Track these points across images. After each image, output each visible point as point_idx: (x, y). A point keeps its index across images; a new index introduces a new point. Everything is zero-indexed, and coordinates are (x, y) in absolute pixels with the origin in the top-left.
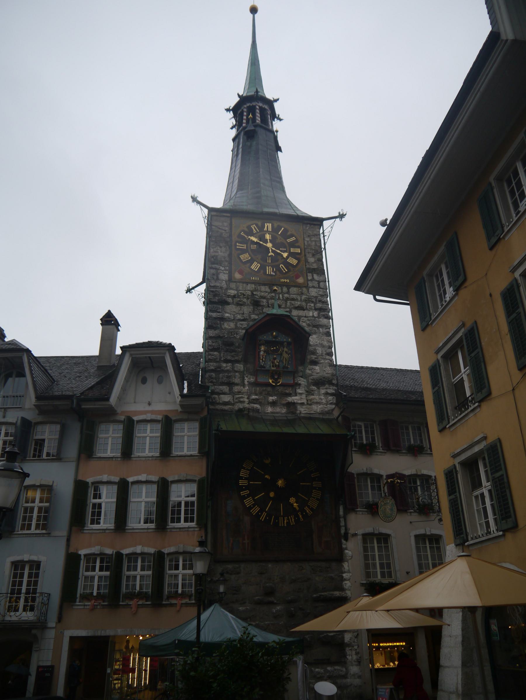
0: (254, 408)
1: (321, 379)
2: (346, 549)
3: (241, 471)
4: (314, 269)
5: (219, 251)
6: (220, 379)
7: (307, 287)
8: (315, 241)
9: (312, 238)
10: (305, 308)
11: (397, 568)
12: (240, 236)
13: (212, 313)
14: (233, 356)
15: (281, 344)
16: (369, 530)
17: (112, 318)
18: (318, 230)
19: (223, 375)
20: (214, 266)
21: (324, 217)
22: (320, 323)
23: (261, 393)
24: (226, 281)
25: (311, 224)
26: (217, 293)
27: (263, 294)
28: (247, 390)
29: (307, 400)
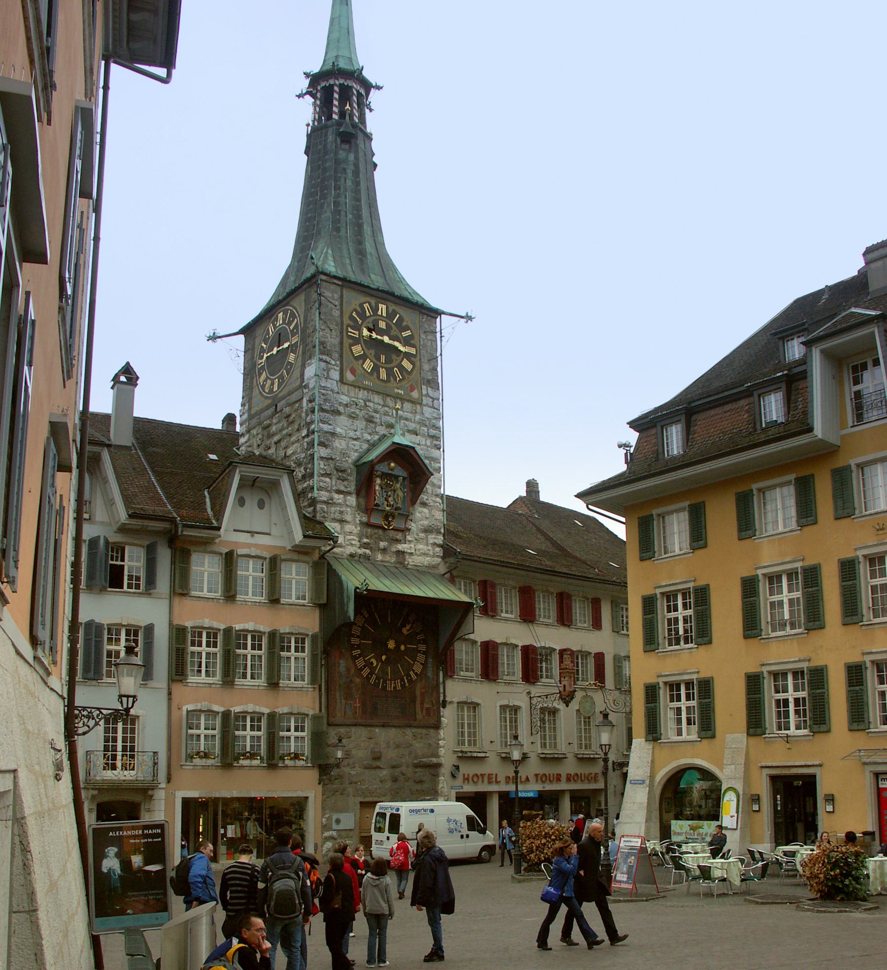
4: (429, 381)
7: (421, 404)
8: (432, 341)
11: (483, 737)
12: (351, 318)
14: (346, 487)
15: (396, 477)
16: (463, 699)
17: (132, 375)
20: (324, 357)
25: (428, 315)
27: (376, 406)
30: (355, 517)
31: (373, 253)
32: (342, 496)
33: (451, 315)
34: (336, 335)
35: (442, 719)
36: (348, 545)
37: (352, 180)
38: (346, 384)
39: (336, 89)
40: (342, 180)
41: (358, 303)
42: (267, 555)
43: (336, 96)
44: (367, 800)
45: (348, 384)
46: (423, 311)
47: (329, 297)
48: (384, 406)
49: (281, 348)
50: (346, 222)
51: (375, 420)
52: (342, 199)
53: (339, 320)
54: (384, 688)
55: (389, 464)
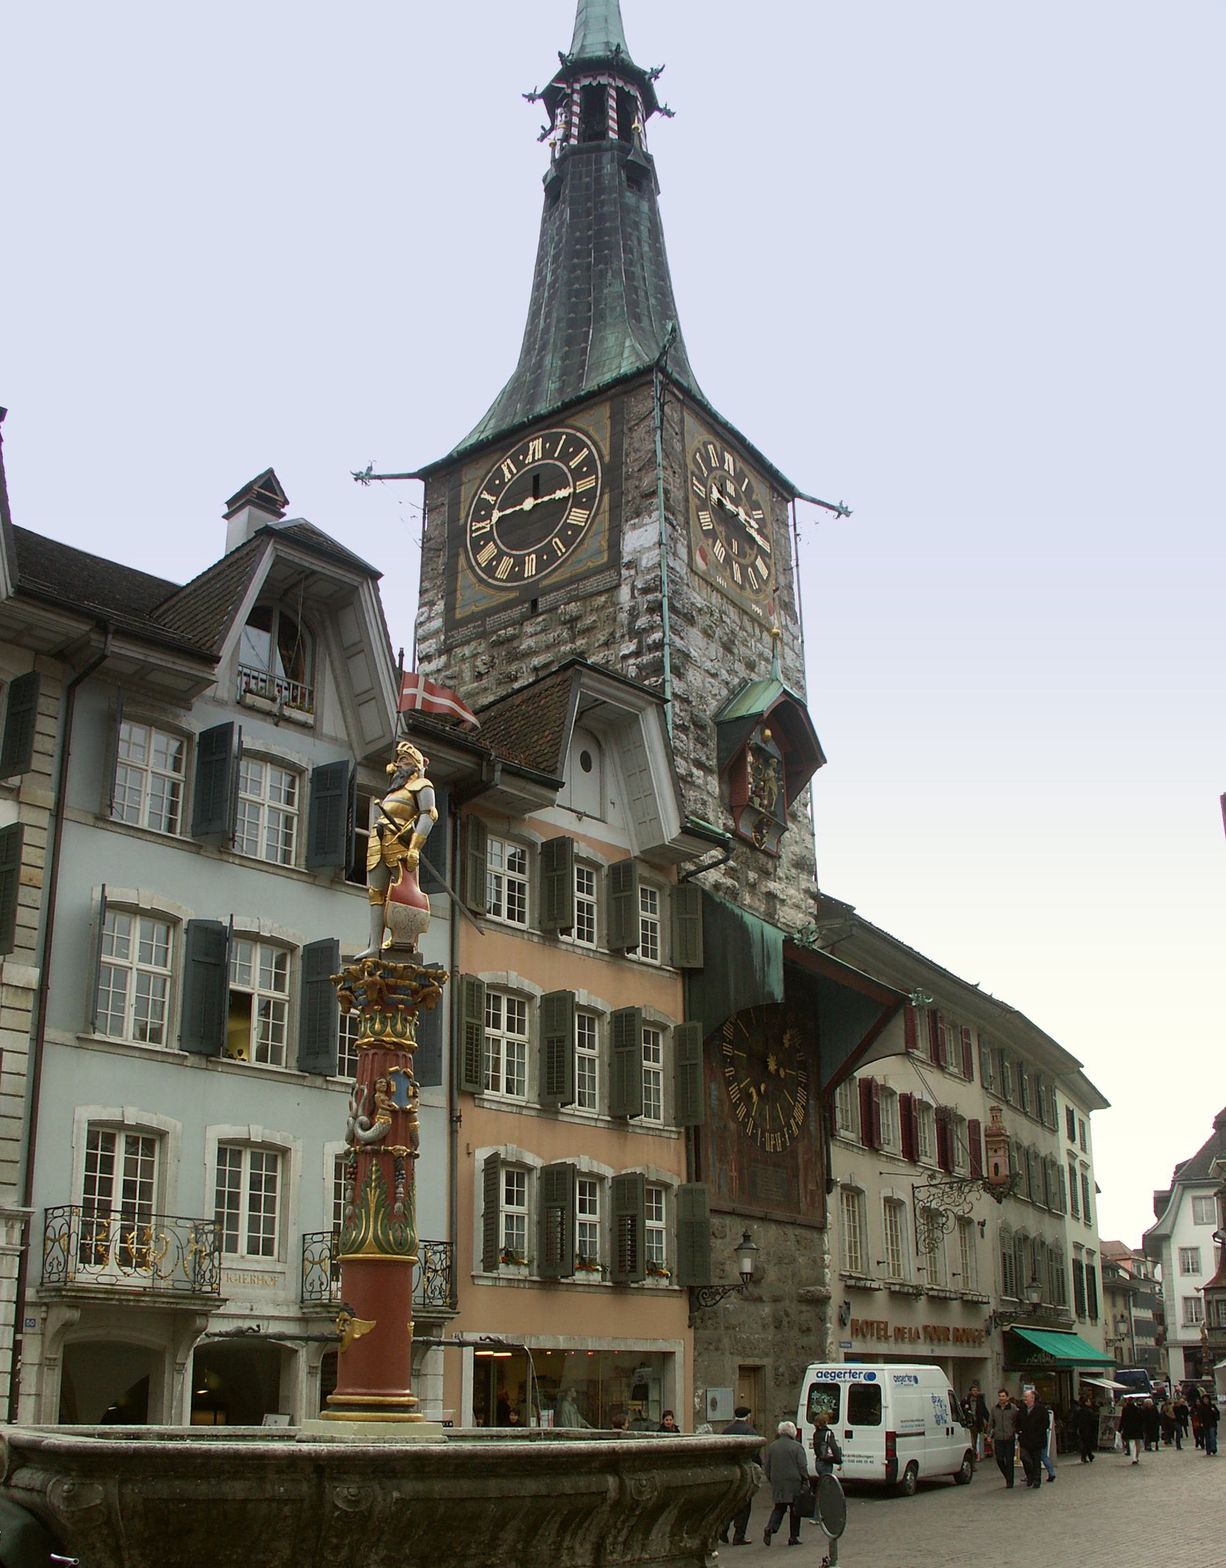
6: (691, 803)
17: (277, 495)
21: (800, 487)
33: (813, 501)
37: (649, 244)
39: (613, 93)
40: (635, 239)
43: (612, 103)
49: (539, 501)
52: (637, 270)
55: (762, 733)
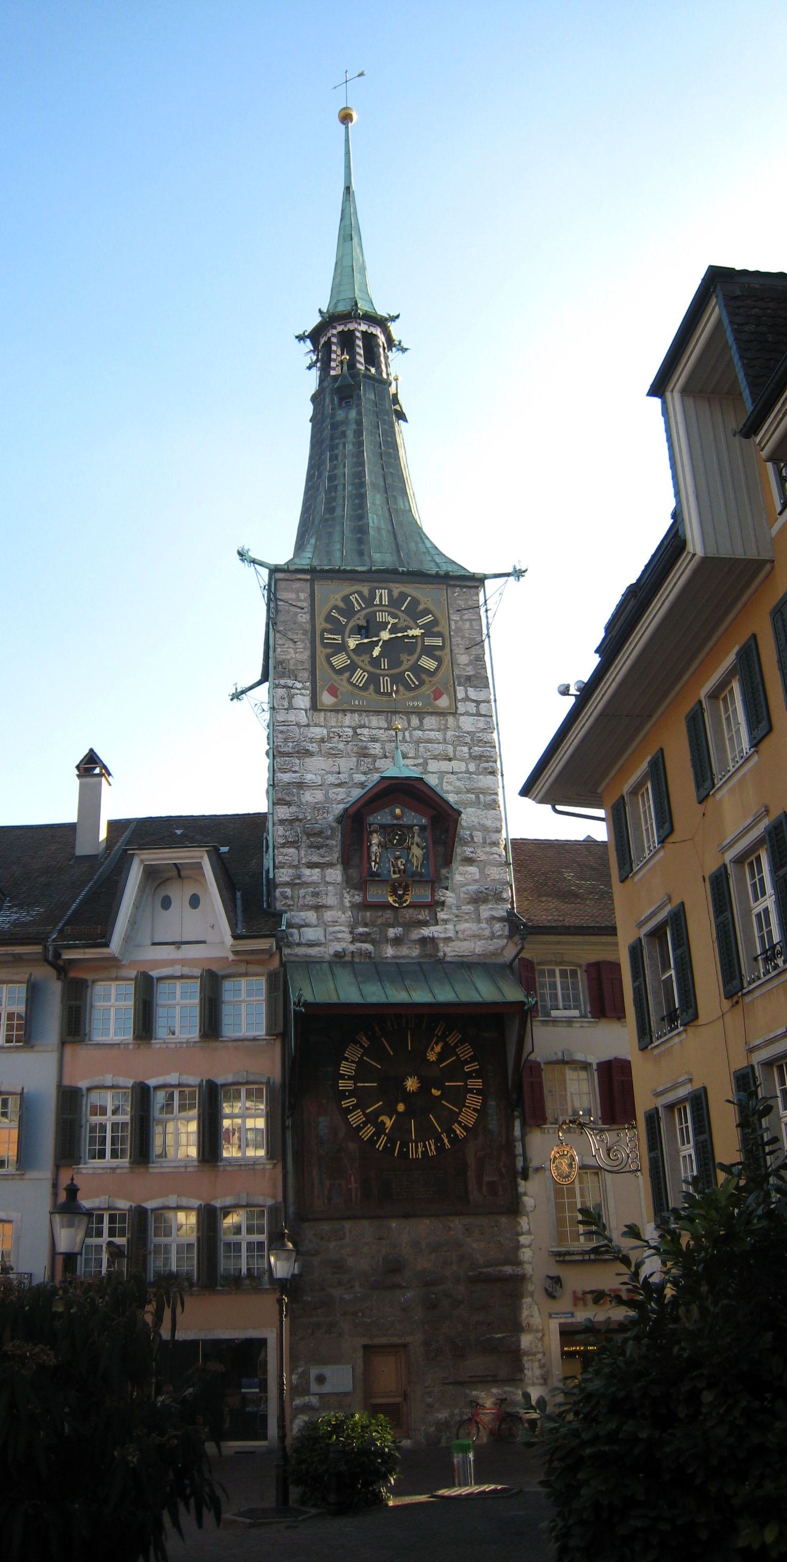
0: (361, 950)
1: (481, 892)
2: (525, 1194)
3: (342, 1065)
4: (469, 678)
5: (291, 651)
7: (454, 714)
8: (471, 620)
9: (464, 614)
10: (452, 756)
13: (282, 775)
15: (410, 827)
18: (474, 598)
19: (306, 890)
20: (282, 682)
22: (480, 785)
23: (372, 924)
24: (306, 710)
25: (462, 587)
26: (291, 734)
27: (374, 732)
28: (349, 917)
29: (457, 932)
30: (342, 897)
31: (383, 526)
32: (317, 871)
34: (304, 648)
35: (525, 1199)
36: (331, 941)
38: (321, 710)
40: (341, 447)
41: (339, 596)
42: (197, 972)
44: (376, 1341)
45: (325, 710)
46: (452, 583)
47: (291, 599)
48: (386, 729)
50: (344, 497)
51: (372, 752)
53: (308, 627)
54: (404, 1155)
